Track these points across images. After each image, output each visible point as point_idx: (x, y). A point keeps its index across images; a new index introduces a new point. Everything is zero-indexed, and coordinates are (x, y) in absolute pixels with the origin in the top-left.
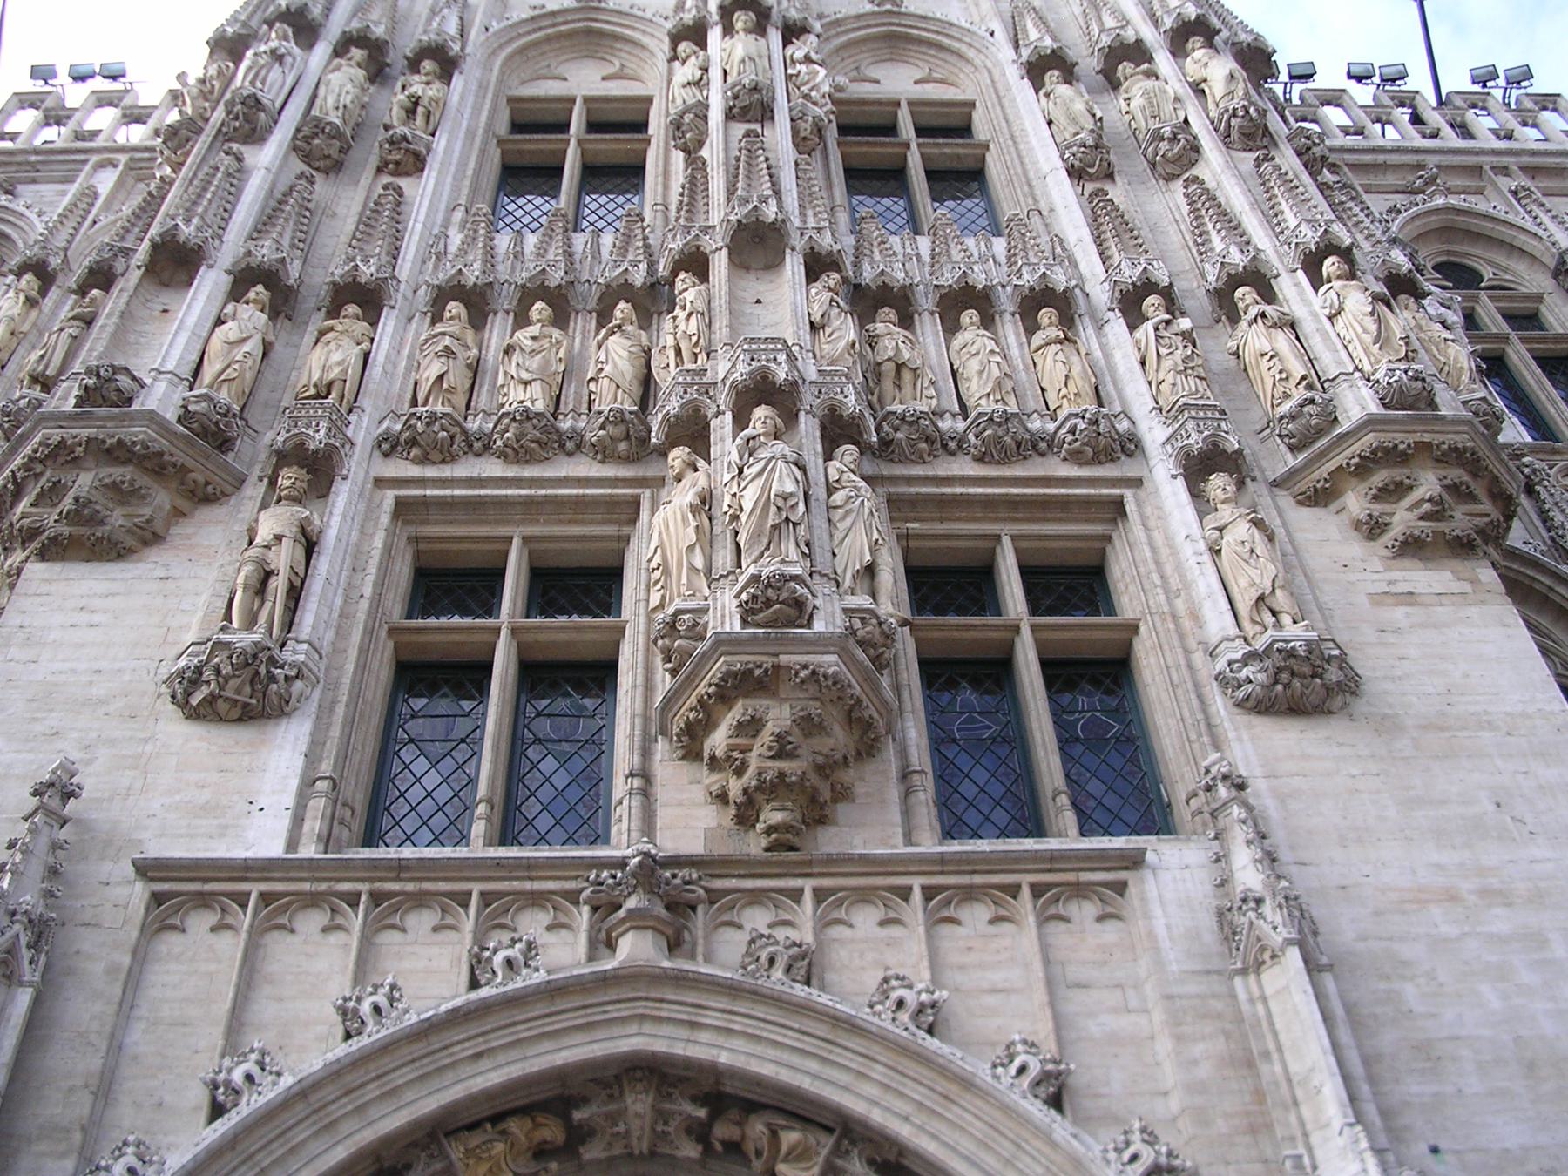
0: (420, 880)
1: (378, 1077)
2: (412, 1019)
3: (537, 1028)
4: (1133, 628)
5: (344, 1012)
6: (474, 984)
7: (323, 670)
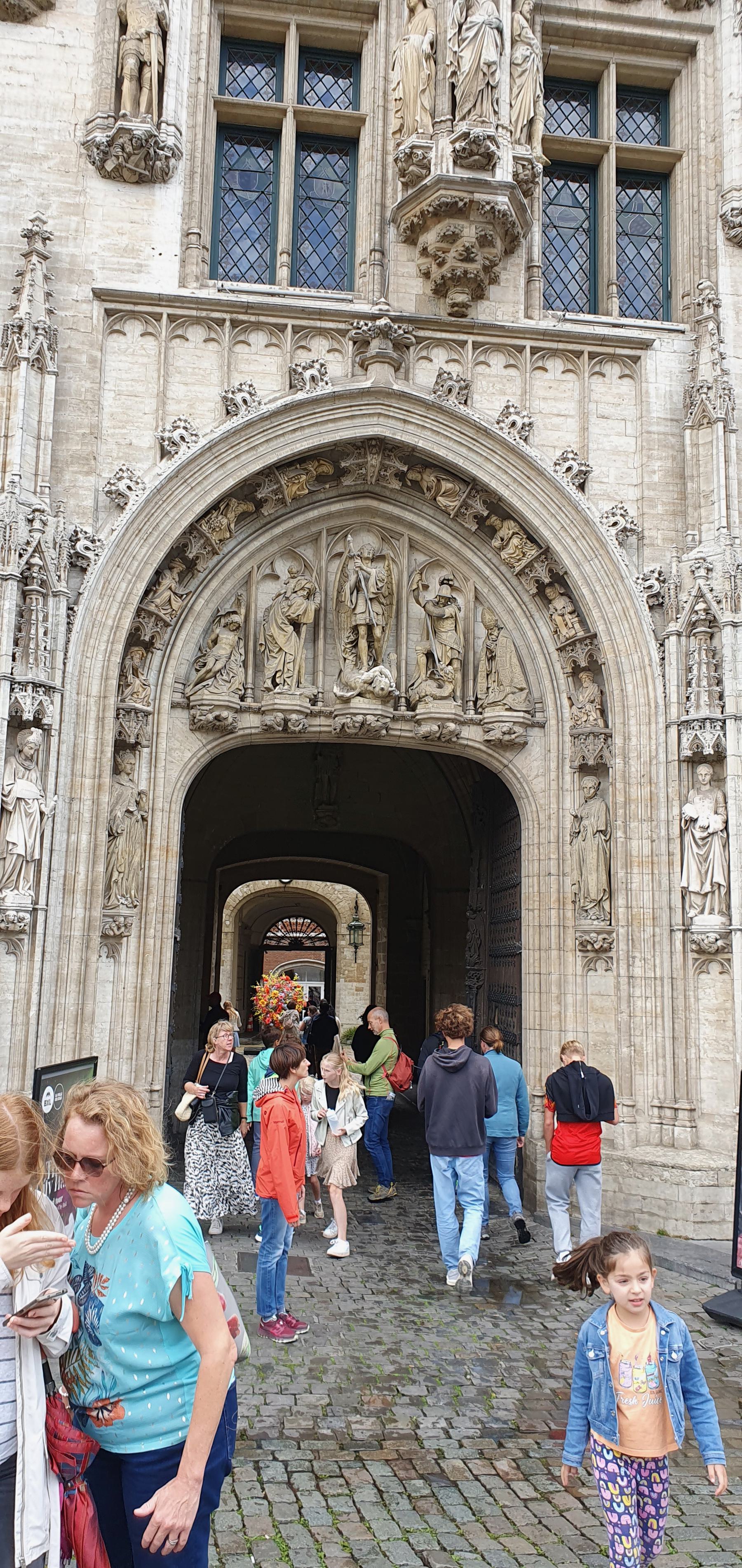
0: (259, 315)
2: (264, 409)
4: (679, 157)
5: (225, 398)
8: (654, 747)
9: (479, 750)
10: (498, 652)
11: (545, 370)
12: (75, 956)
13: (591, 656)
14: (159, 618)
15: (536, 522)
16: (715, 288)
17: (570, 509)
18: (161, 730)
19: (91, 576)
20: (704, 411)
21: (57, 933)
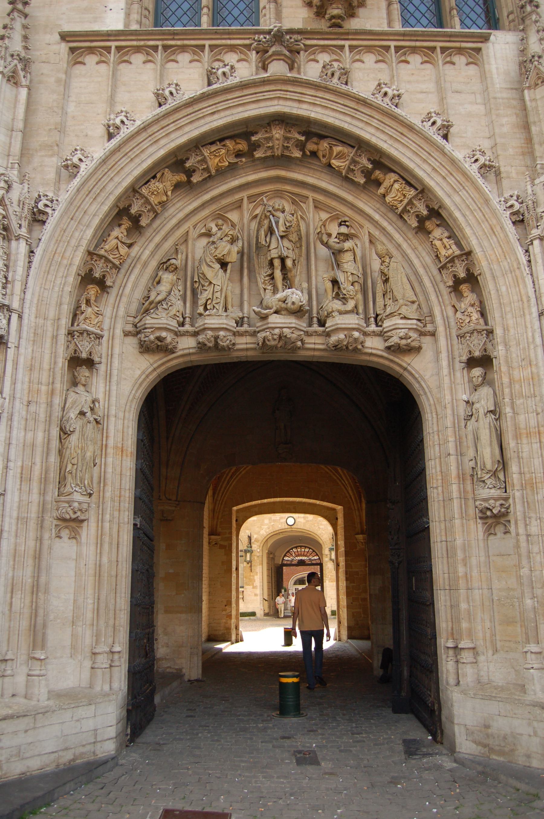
1: (174, 122)
2: (186, 97)
3: (236, 102)
5: (157, 95)
6: (209, 84)
8: (530, 334)
9: (381, 357)
10: (391, 274)
11: (407, 62)
12: (32, 535)
13: (468, 270)
14: (107, 260)
15: (411, 165)
17: (438, 154)
18: (114, 352)
19: (49, 226)
20: (537, 74)
21: (15, 514)
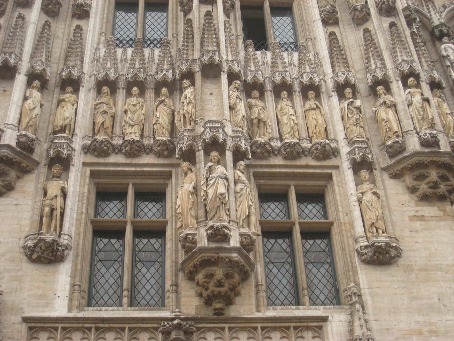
0: (110, 323)
4: (332, 224)
7: (73, 243)
16: (357, 284)
